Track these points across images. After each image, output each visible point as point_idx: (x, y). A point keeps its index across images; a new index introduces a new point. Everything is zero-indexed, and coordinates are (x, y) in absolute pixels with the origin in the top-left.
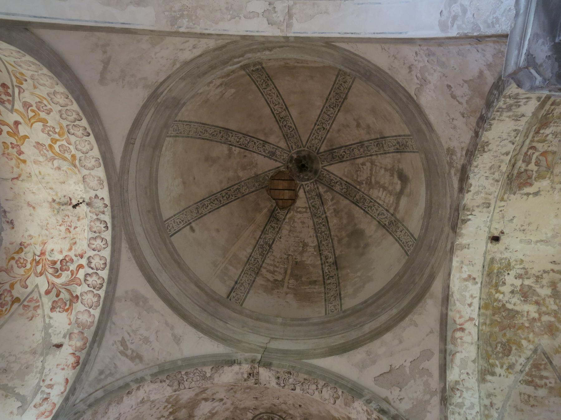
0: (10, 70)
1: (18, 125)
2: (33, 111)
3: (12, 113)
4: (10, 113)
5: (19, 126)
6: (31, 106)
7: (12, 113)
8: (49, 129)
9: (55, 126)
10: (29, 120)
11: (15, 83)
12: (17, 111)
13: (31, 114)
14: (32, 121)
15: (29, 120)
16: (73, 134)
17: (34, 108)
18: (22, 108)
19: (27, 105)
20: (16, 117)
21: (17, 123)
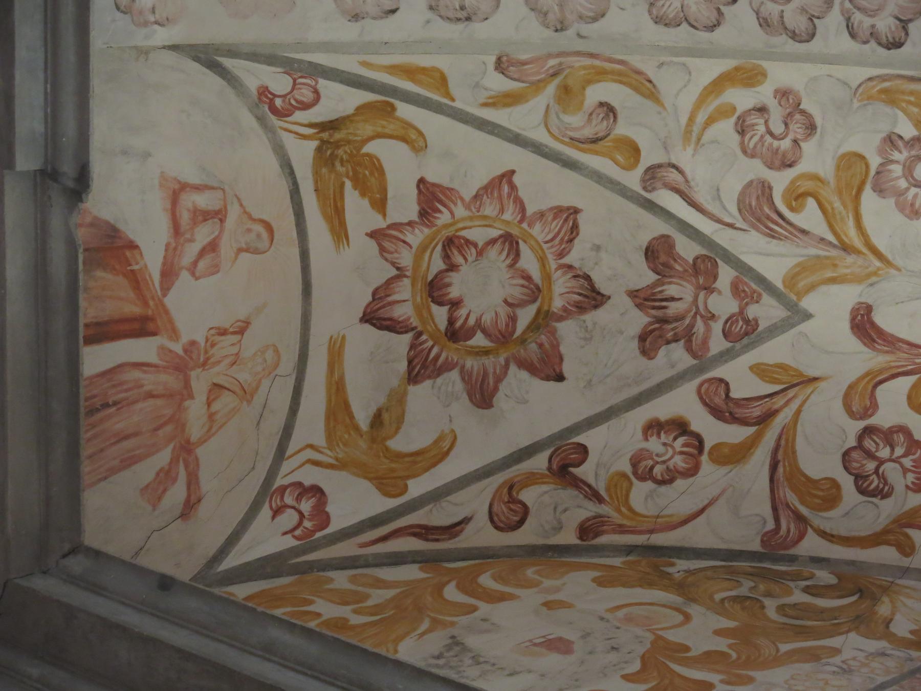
0: (541, 136)
1: (873, 324)
2: (796, 198)
3: (808, 316)
4: (804, 327)
5: (879, 318)
6: (765, 189)
7: (808, 316)
8: (897, 170)
9: (885, 128)
10: (846, 248)
11: (633, 180)
12: (791, 279)
13: (809, 217)
14: (852, 235)
15: (846, 248)
16: (904, 24)
17: (780, 181)
18: (774, 246)
19: (759, 209)
20: (830, 307)
21: (864, 325)
